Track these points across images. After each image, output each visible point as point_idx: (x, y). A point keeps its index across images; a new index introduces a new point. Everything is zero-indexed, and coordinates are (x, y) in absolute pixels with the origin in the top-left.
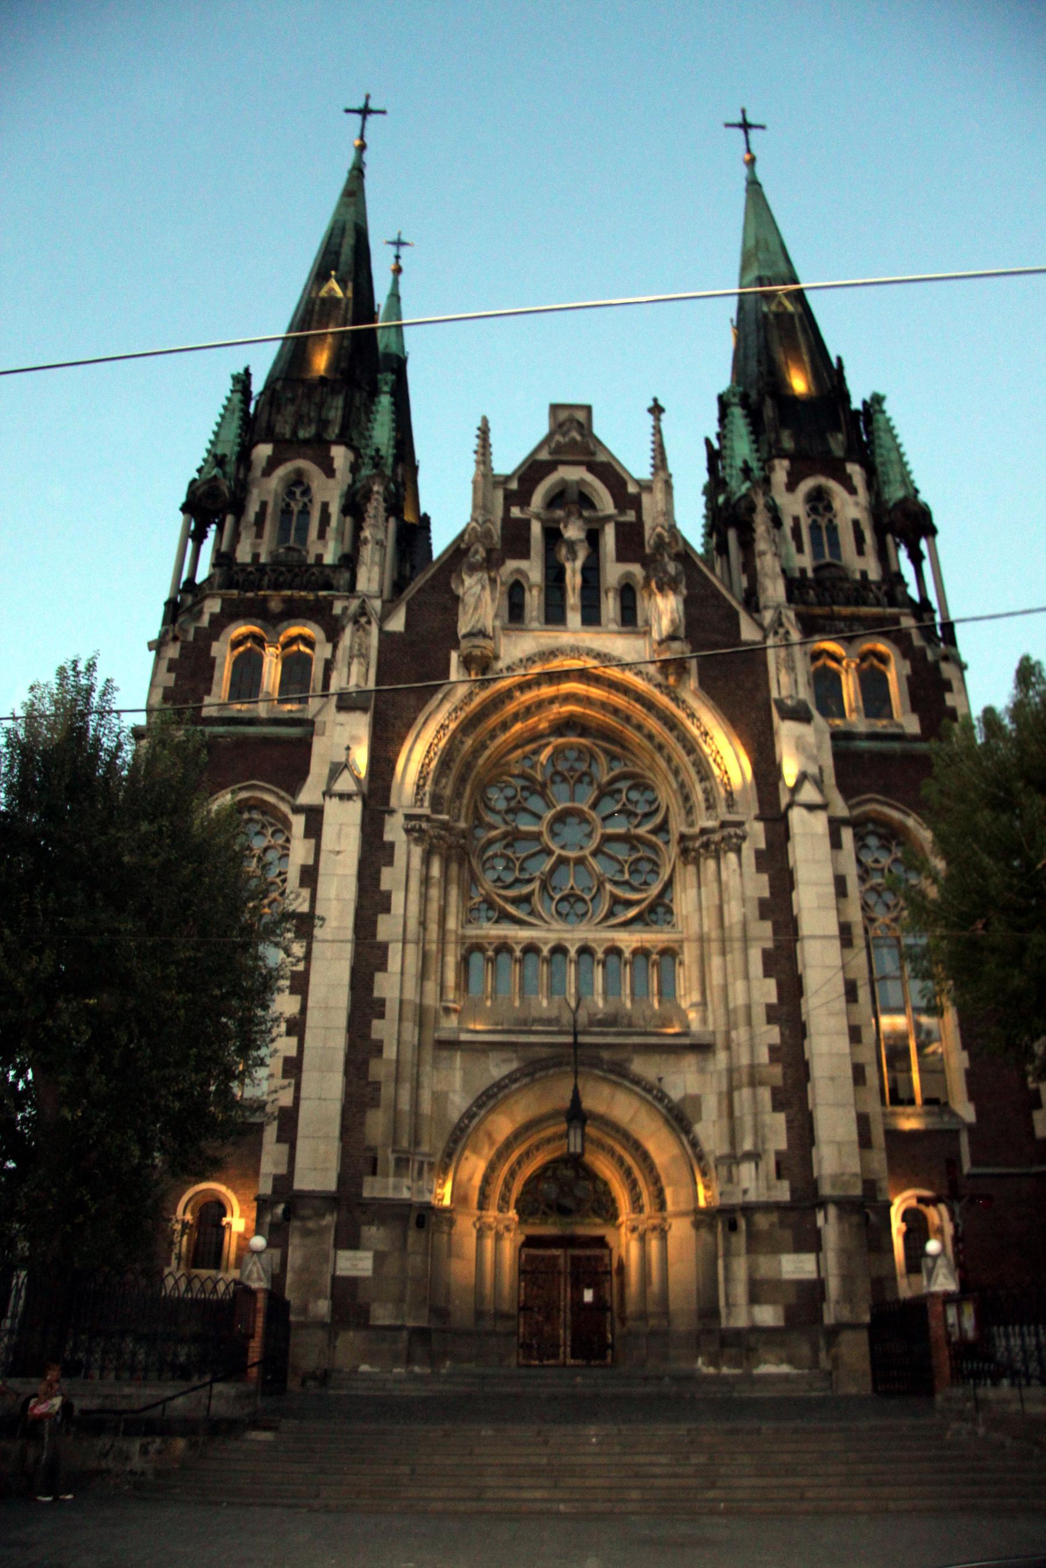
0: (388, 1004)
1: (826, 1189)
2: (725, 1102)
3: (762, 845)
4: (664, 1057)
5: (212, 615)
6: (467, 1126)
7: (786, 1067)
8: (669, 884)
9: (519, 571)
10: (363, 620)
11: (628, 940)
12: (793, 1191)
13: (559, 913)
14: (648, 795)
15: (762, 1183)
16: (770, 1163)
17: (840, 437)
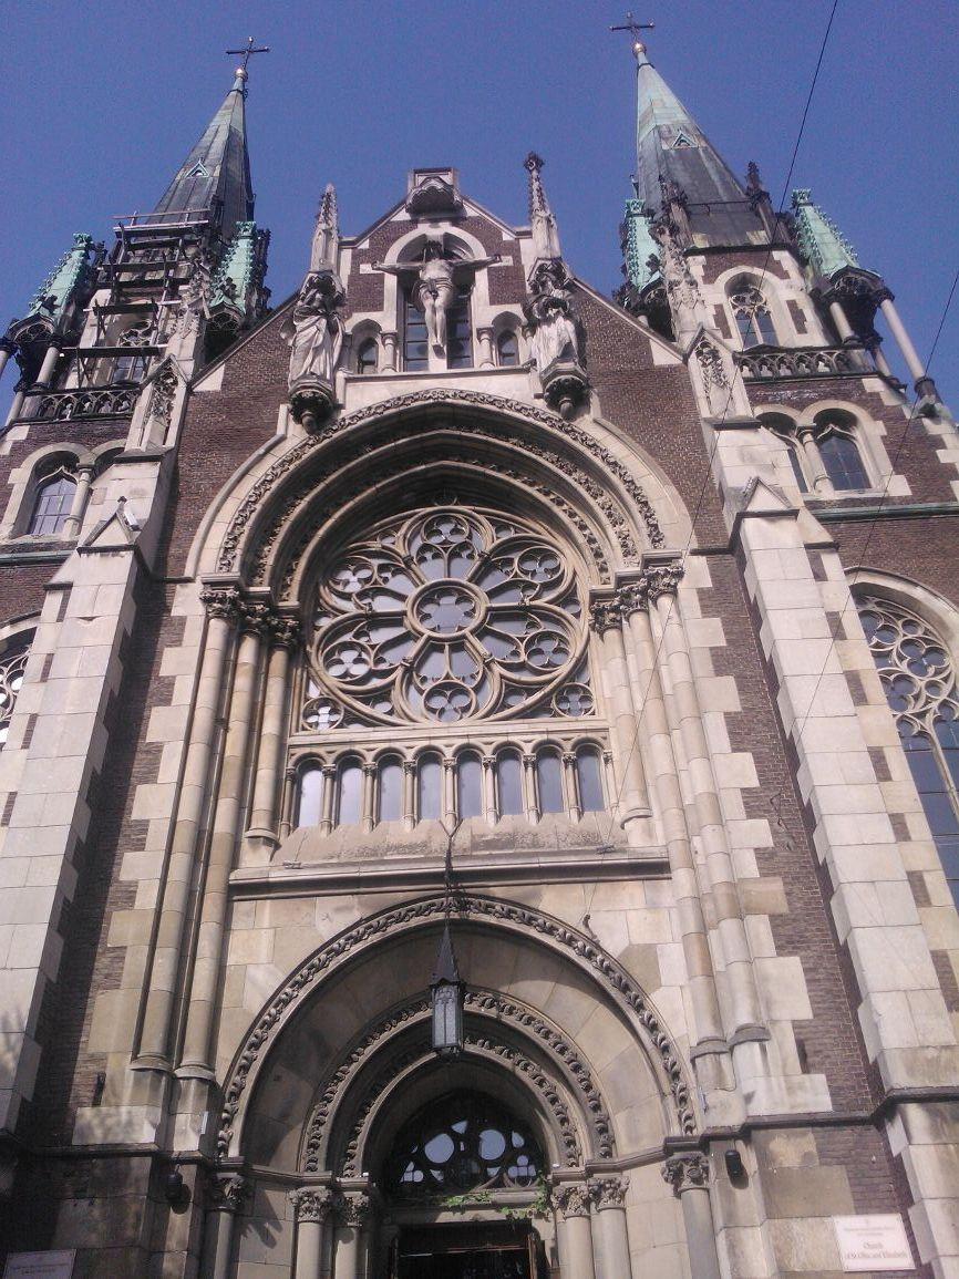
0: (151, 828)
1: (899, 1078)
2: (696, 949)
3: (708, 583)
4: (591, 886)
5: (15, 443)
6: (275, 1020)
7: (791, 881)
8: (582, 664)
9: (371, 327)
10: (170, 381)
11: (527, 734)
12: (835, 1093)
13: (433, 711)
14: (550, 564)
15: (777, 1081)
16: (785, 1043)
17: (763, 233)
